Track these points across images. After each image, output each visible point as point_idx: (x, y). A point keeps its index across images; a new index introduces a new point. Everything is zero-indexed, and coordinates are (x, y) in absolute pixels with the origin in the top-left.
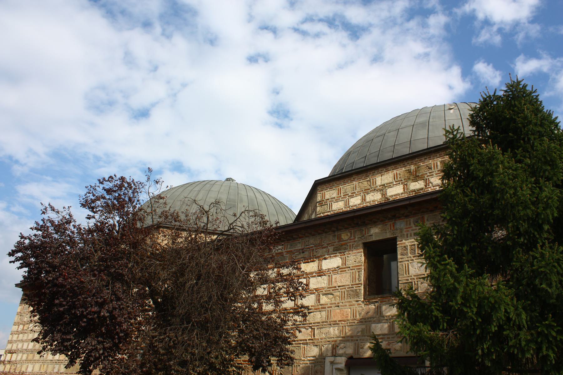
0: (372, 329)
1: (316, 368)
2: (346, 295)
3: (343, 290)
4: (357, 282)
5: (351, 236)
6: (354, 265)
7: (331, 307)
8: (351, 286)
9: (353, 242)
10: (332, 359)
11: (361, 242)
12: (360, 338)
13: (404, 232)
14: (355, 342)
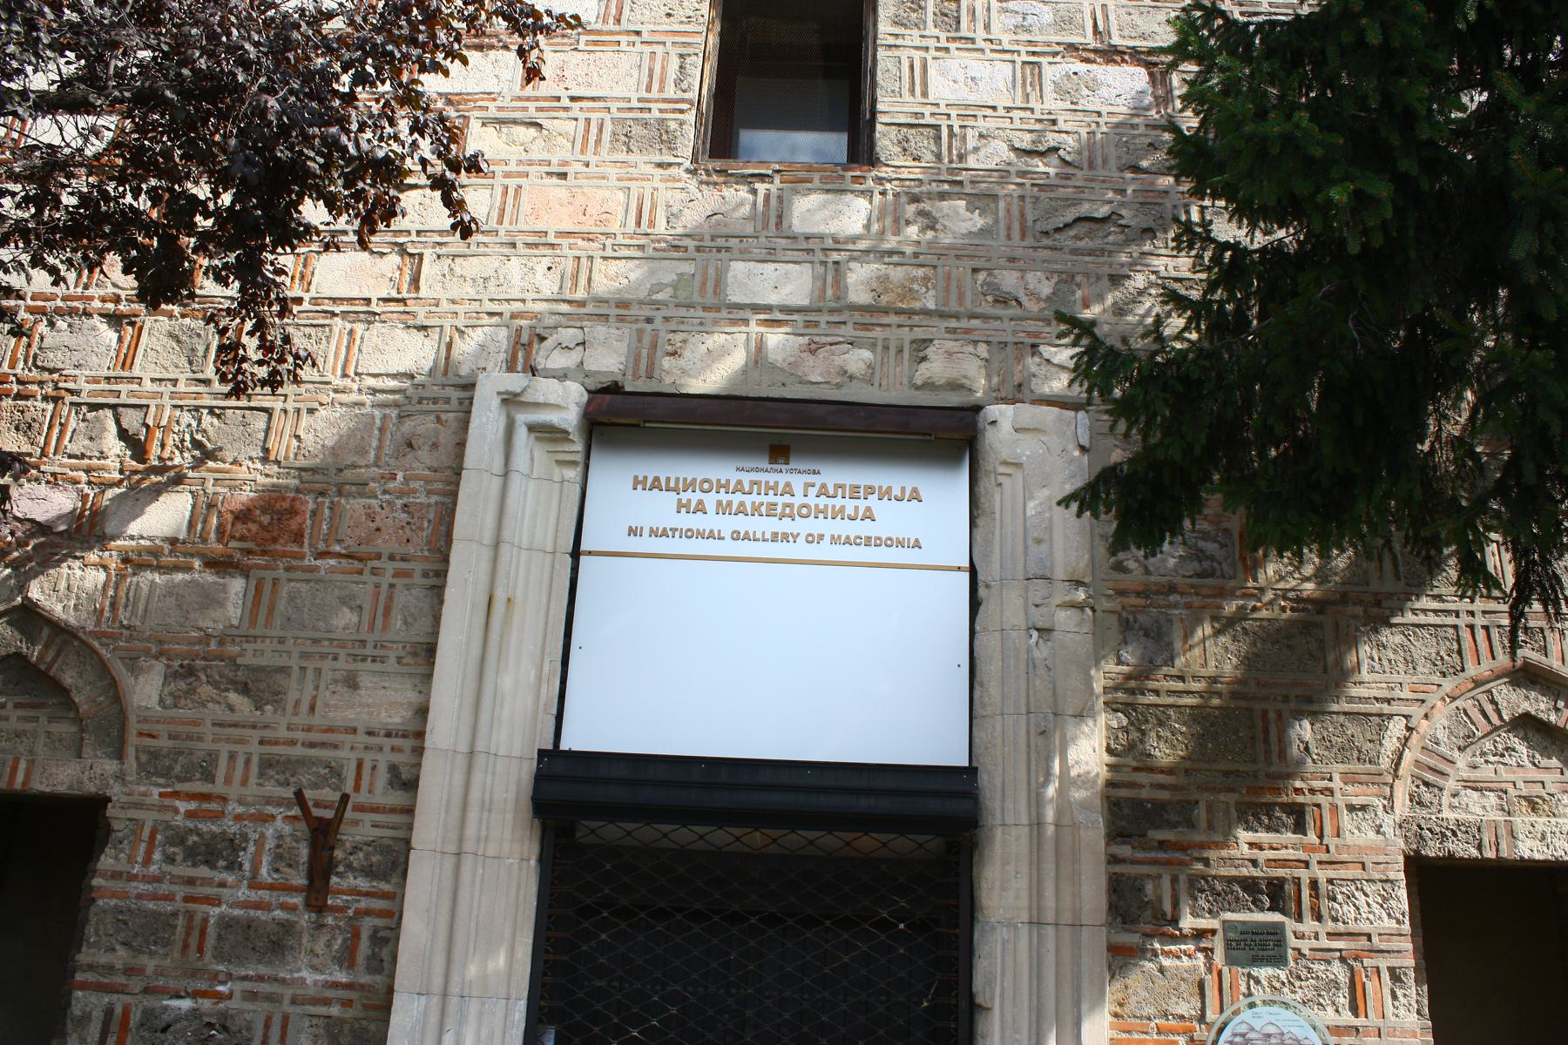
0: (730, 280)
1: (408, 426)
2: (606, 136)
3: (594, 116)
4: (670, 92)
8: (635, 104)
10: (516, 382)
14: (635, 326)
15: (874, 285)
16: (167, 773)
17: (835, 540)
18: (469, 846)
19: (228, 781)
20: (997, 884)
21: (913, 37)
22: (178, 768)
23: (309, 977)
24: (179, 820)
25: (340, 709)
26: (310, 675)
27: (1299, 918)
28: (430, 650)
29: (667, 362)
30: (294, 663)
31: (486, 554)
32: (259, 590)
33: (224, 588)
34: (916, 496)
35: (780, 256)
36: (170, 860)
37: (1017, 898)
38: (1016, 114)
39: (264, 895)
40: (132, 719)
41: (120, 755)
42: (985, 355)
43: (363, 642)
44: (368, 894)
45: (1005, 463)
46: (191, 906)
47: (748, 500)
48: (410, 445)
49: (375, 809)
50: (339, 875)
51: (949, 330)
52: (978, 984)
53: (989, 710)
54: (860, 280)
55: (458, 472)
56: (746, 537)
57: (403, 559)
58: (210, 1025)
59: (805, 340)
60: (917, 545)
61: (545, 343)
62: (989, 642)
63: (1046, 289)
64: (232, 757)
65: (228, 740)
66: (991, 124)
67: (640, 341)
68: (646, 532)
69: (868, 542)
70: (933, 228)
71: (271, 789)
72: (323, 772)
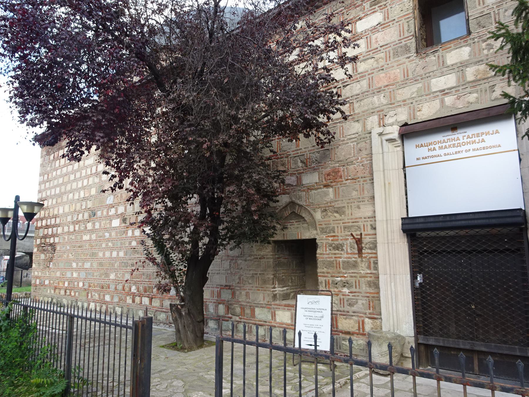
1: (359, 146)
4: (406, 35)
6: (402, 15)
7: (373, 73)
10: (380, 130)
12: (416, 100)
14: (408, 106)
15: (475, 73)
16: (326, 232)
17: (474, 150)
18: (390, 241)
19: (338, 232)
23: (362, 272)
24: (330, 242)
25: (358, 214)
26: (350, 207)
28: (373, 197)
29: (418, 113)
30: (346, 205)
34: (497, 132)
35: (445, 74)
39: (350, 255)
40: (317, 222)
41: (316, 230)
44: (371, 253)
47: (447, 144)
49: (369, 235)
54: (470, 73)
56: (448, 154)
60: (499, 146)
64: (338, 227)
68: (421, 159)
69: (484, 148)
70: (492, 48)
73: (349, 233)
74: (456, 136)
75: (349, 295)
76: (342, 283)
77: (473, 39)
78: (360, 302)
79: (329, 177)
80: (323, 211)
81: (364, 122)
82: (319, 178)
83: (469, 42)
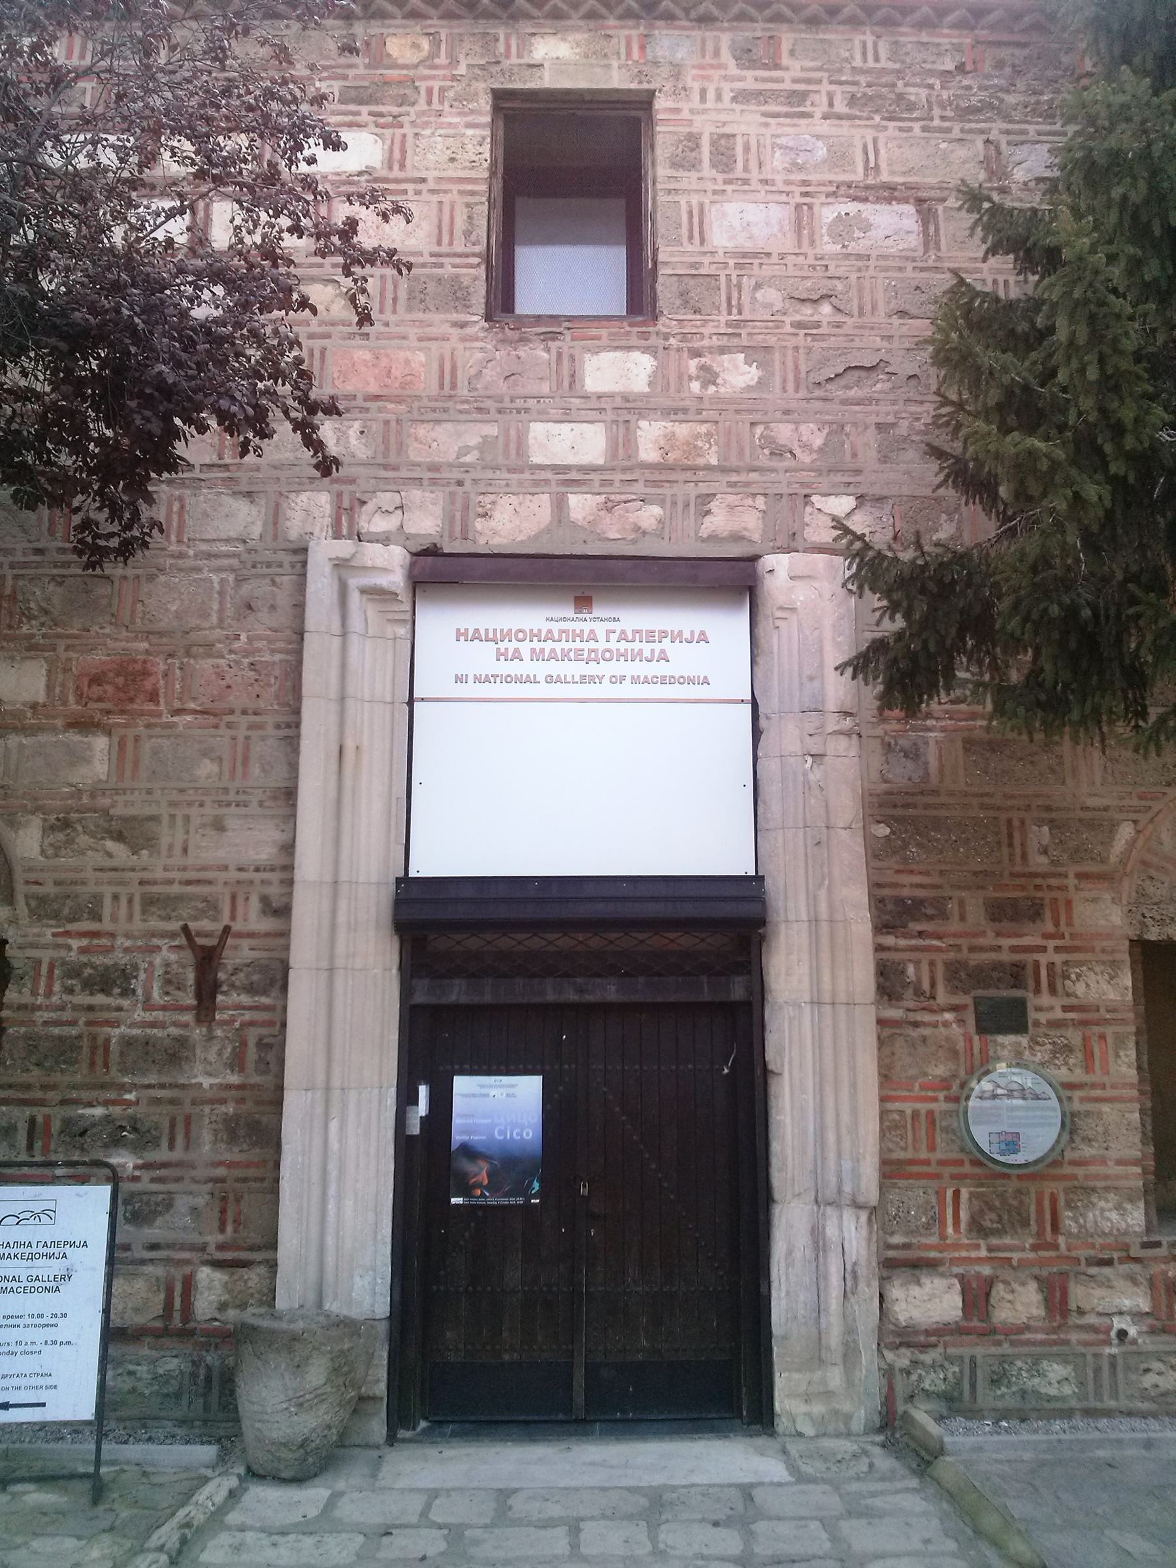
0: (531, 441)
1: (245, 589)
4: (459, 247)
5: (434, 54)
6: (451, 173)
7: (327, 336)
9: (444, 78)
10: (344, 548)
11: (481, 86)
12: (474, 474)
13: (689, 79)
14: (448, 489)
15: (662, 443)
16: (56, 916)
17: (635, 680)
18: (340, 962)
19: (114, 919)
20: (783, 971)
21: (689, 179)
22: (66, 911)
23: (206, 1082)
26: (179, 822)
27: (1037, 991)
28: (290, 795)
29: (479, 524)
30: (164, 811)
31: (334, 707)
32: (122, 745)
33: (90, 747)
34: (703, 638)
35: (574, 415)
36: (70, 991)
37: (800, 981)
38: (790, 259)
39: (159, 1015)
42: (762, 507)
43: (226, 790)
44: (250, 1008)
45: (781, 608)
46: (95, 1029)
47: (558, 646)
48: (250, 607)
49: (251, 935)
50: (223, 993)
51: (731, 484)
52: (770, 1055)
53: (771, 825)
55: (300, 634)
56: (559, 680)
57: (255, 714)
58: (123, 1128)
59: (601, 498)
60: (706, 681)
61: (364, 508)
62: (769, 767)
63: (818, 442)
64: (116, 897)
65: (110, 883)
66: (767, 271)
67: (453, 503)
68: (471, 679)
69: (663, 680)
70: (714, 384)
71: (155, 924)
72: (201, 905)
73: (175, 926)
74: (587, 627)
75: (136, 1179)
76: (109, 1128)
77: (666, 337)
78: (182, 1203)
79: (96, 690)
80: (52, 828)
81: (277, 505)
82: (49, 688)
83: (654, 340)
